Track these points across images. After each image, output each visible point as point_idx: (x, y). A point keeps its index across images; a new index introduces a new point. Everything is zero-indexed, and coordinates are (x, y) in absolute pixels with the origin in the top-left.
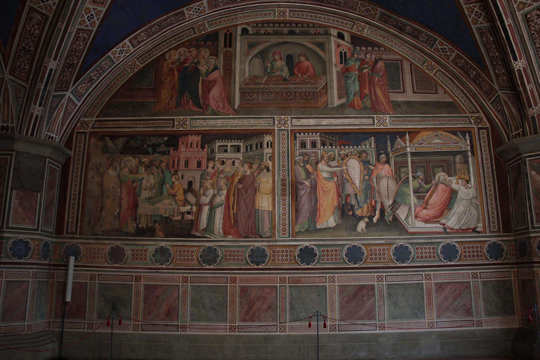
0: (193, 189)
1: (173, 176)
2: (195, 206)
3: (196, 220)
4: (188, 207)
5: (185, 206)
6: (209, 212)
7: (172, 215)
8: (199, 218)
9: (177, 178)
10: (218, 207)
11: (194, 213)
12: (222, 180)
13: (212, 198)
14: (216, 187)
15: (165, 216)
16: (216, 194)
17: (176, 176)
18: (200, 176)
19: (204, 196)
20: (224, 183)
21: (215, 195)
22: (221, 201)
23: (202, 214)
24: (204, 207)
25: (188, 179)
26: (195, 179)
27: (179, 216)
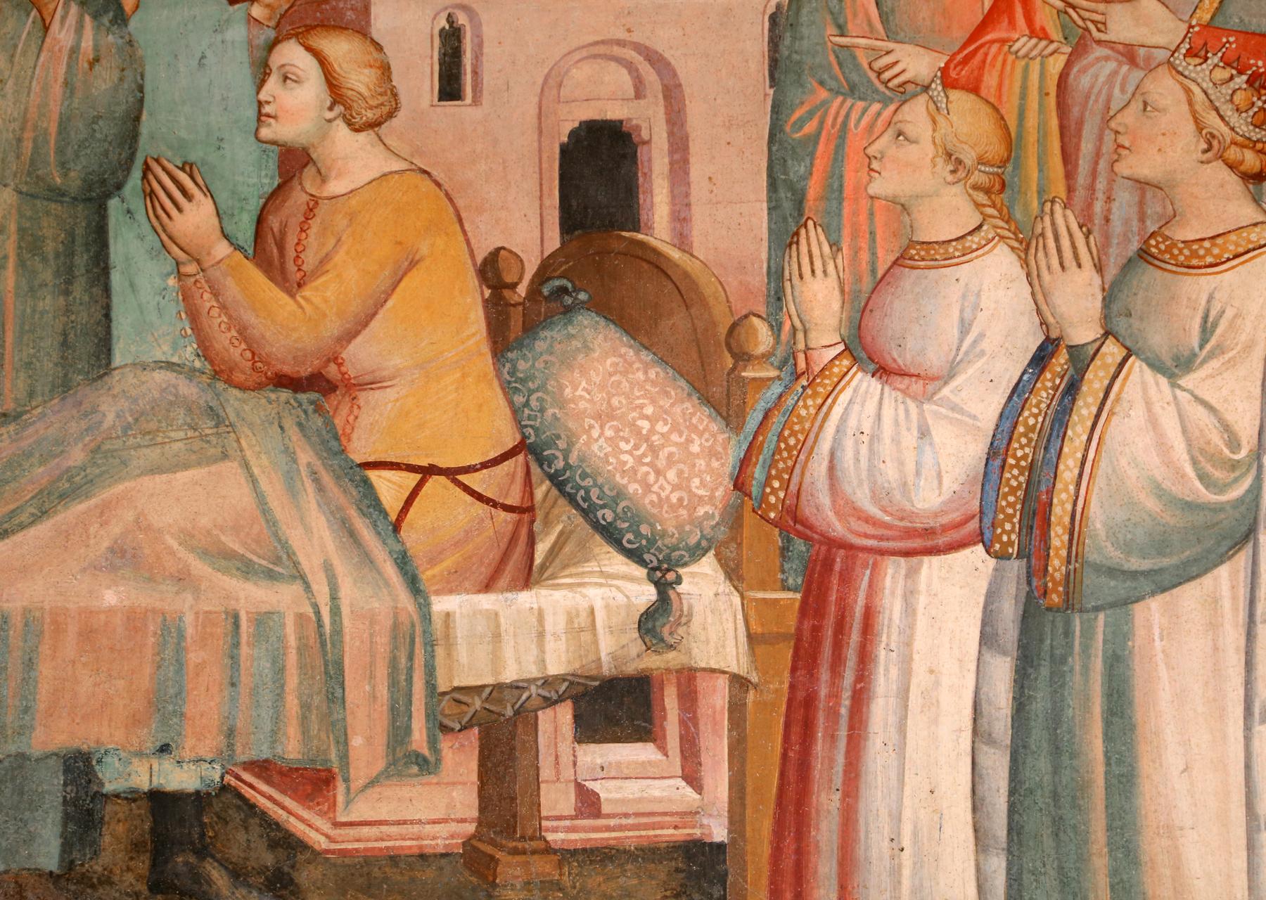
0: (655, 262)
1: (292, 54)
2: (733, 573)
3: (762, 826)
4: (596, 596)
5: (528, 578)
6: (1002, 670)
7: (292, 749)
8: (827, 802)
9: (359, 80)
10: (1165, 581)
11: (716, 698)
12: (1164, 89)
13: (1031, 417)
14: (1066, 220)
15: (142, 776)
16: (1083, 332)
17: (339, 48)
18: (755, 44)
19: (863, 385)
20: (1212, 147)
21: (1081, 359)
22: (1199, 454)
23: (881, 711)
24: (893, 572)
25: (553, 82)
26: (673, 96)
27: (426, 765)
